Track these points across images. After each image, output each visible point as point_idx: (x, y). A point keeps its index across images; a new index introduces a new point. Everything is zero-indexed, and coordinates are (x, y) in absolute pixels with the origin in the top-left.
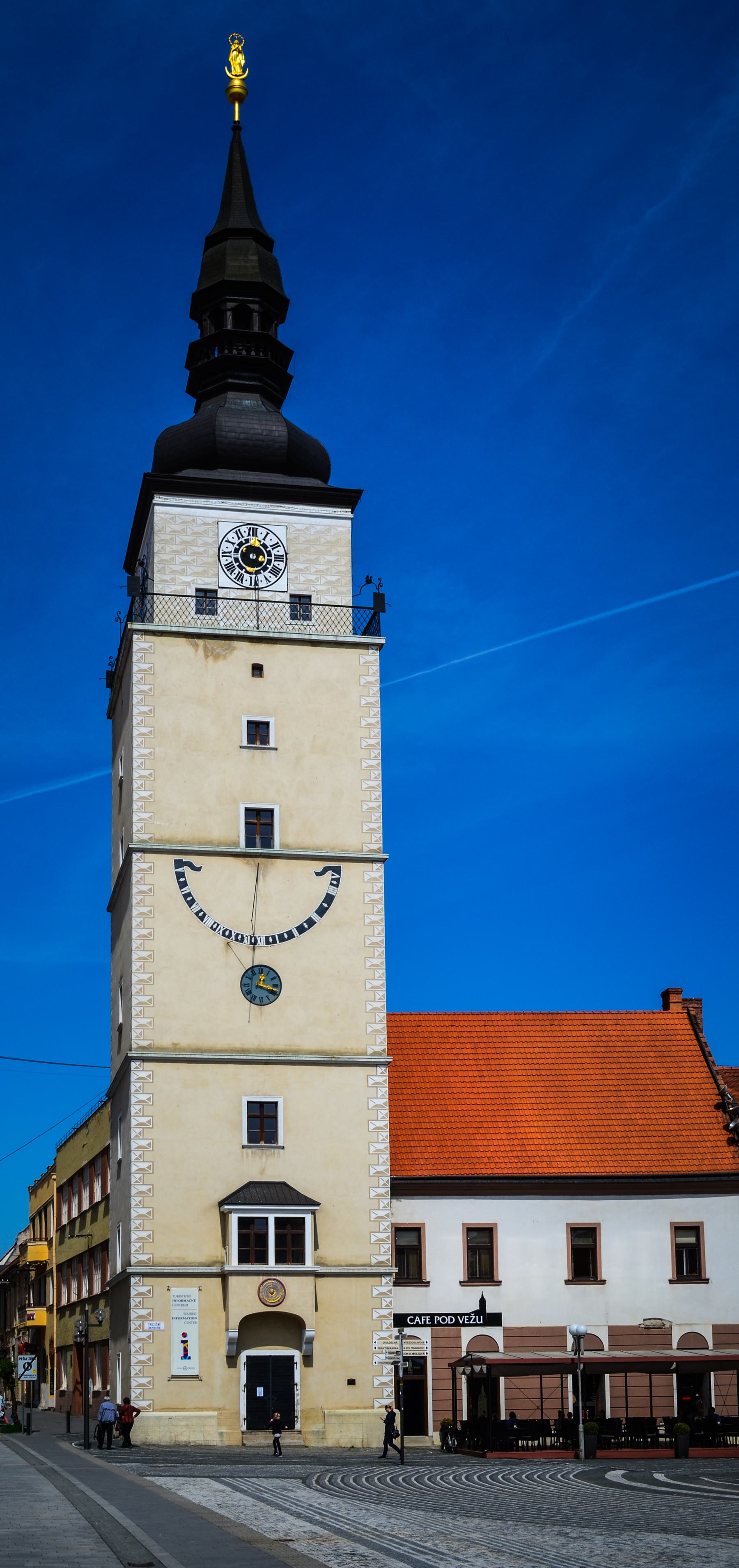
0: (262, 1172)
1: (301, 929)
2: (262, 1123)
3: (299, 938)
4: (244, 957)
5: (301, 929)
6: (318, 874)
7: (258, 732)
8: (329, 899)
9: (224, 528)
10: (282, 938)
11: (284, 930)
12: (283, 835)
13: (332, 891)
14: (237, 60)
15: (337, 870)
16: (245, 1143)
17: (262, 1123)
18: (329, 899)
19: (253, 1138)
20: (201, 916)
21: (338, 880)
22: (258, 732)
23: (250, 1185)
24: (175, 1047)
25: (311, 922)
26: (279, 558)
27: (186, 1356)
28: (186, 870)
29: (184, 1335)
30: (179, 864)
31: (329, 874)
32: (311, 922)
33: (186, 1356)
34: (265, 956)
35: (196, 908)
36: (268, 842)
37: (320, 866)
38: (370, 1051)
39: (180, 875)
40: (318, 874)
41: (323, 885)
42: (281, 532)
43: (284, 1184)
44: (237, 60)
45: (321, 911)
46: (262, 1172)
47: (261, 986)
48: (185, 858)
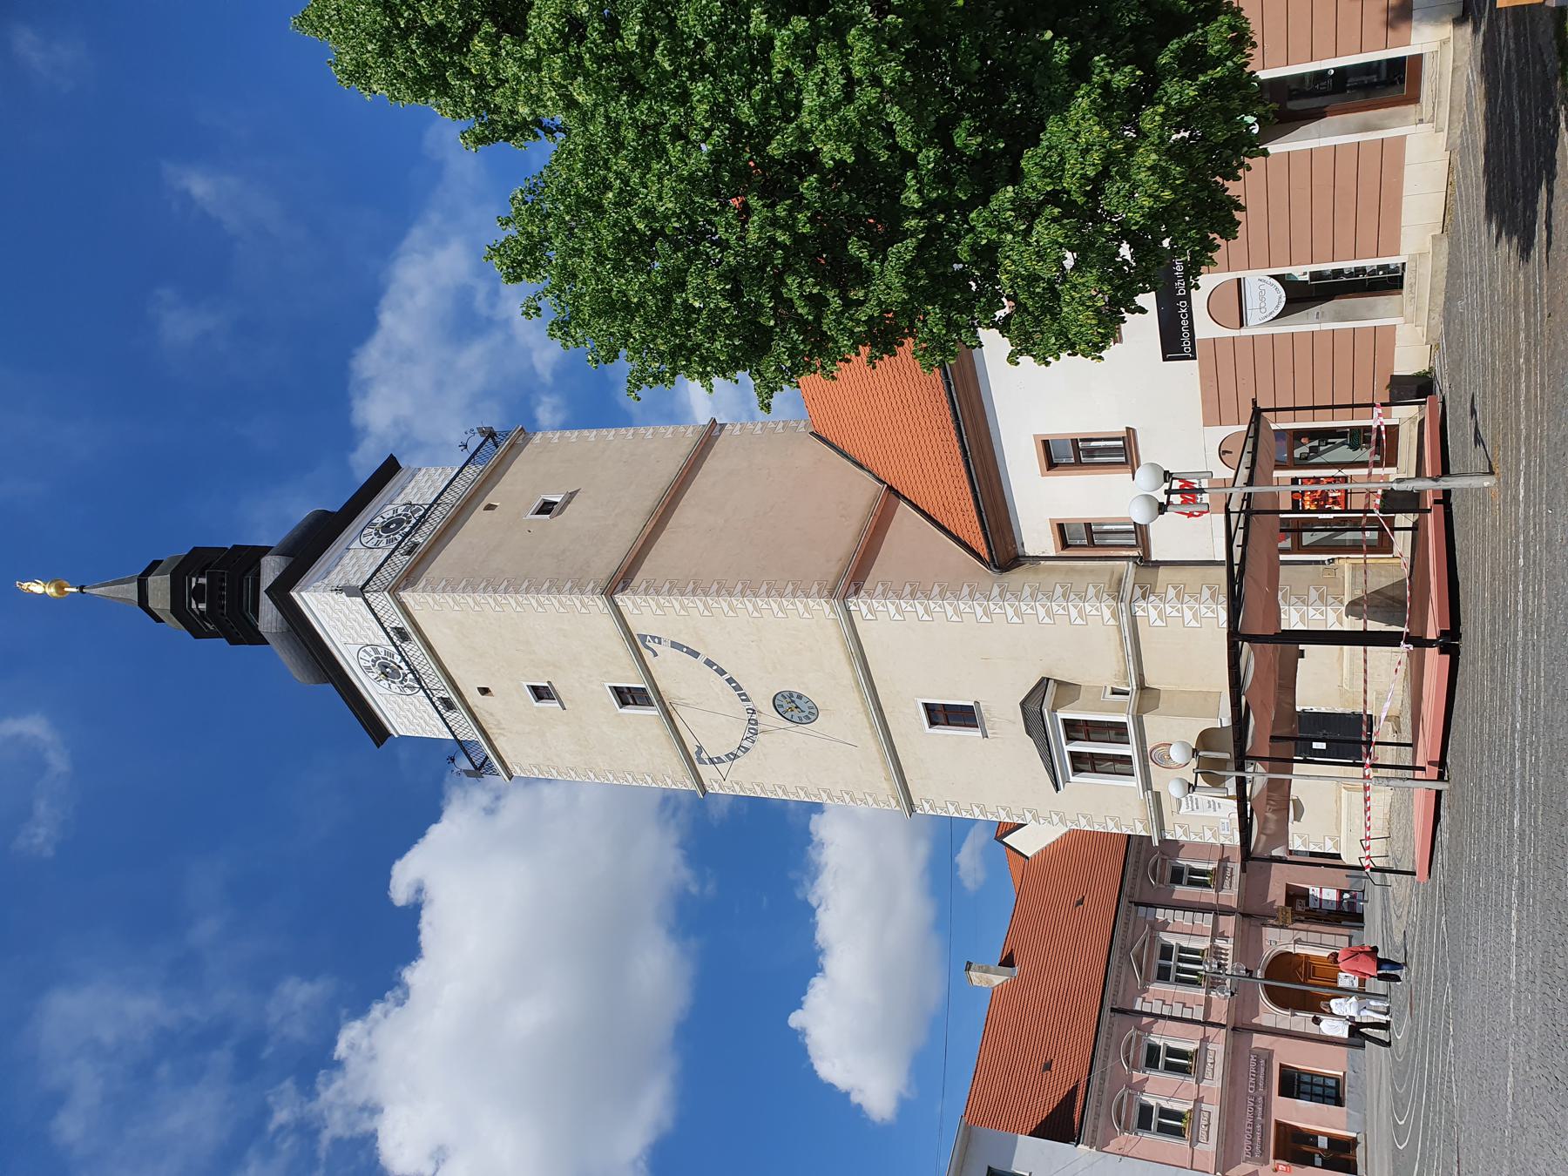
1: (721, 672)
3: (731, 673)
5: (721, 672)
6: (656, 655)
7: (540, 693)
8: (674, 645)
9: (382, 691)
10: (738, 688)
14: (37, 588)
15: (643, 638)
18: (674, 645)
22: (540, 693)
23: (1028, 733)
25: (709, 663)
26: (376, 652)
30: (702, 762)
31: (651, 645)
32: (709, 663)
37: (647, 654)
38: (832, 616)
40: (656, 655)
41: (664, 650)
44: (37, 588)
45: (696, 654)
47: (793, 707)
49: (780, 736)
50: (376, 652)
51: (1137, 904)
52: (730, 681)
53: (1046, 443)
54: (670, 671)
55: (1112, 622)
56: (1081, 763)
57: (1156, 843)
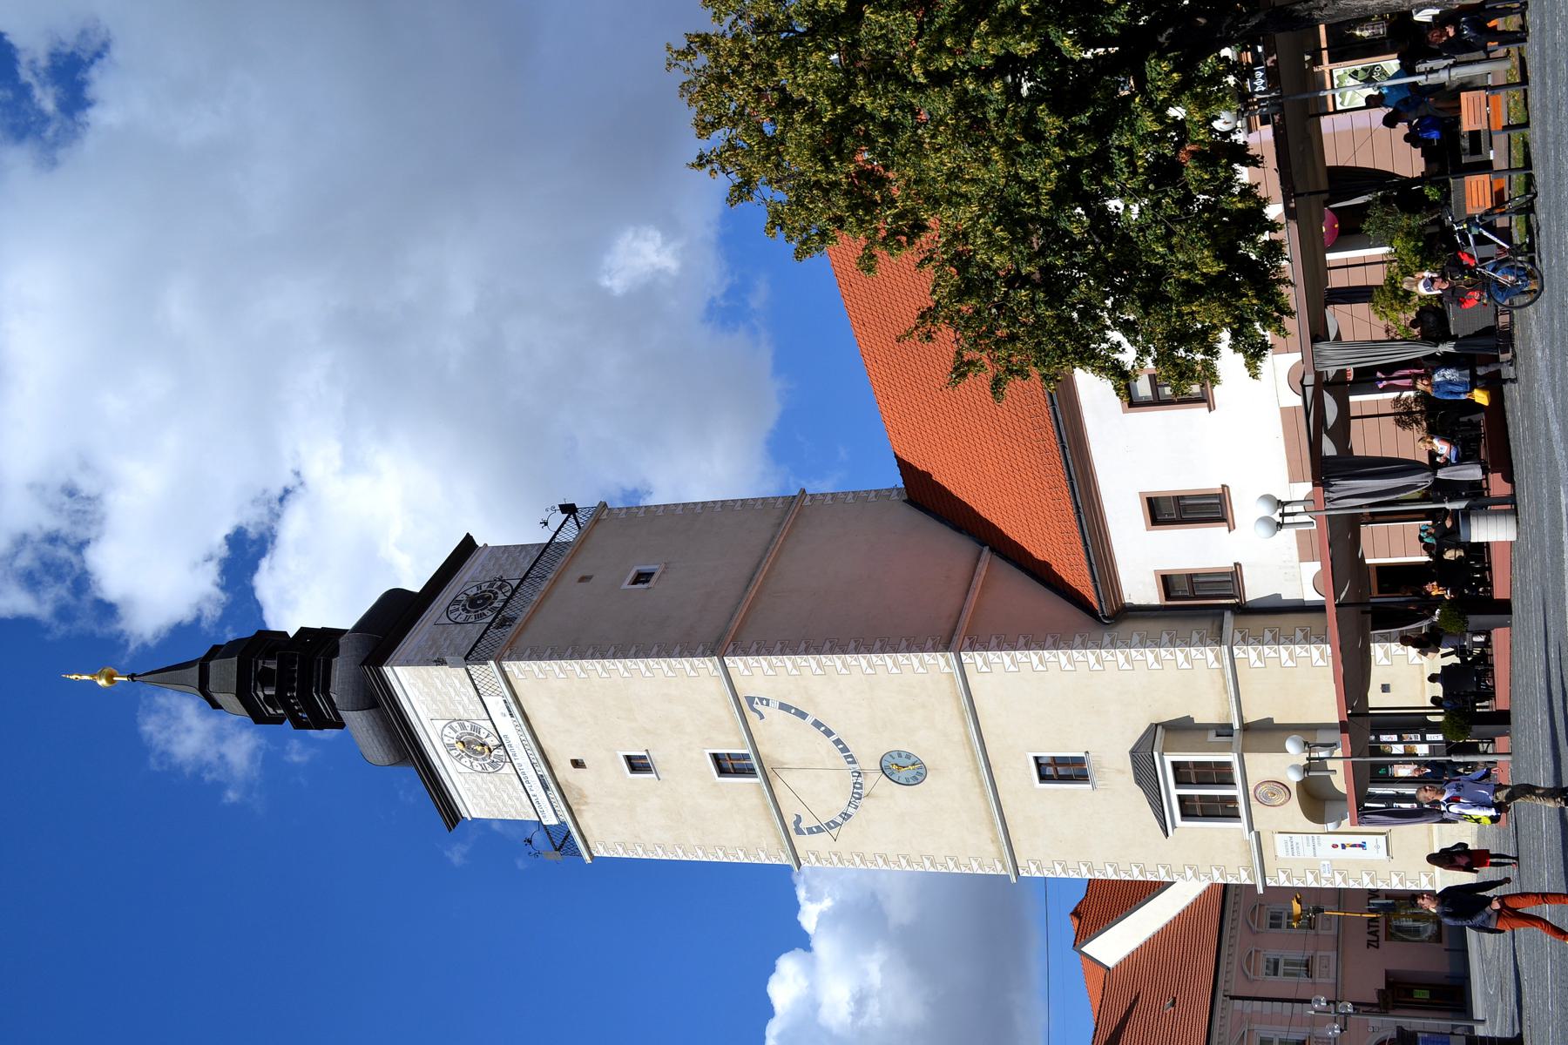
0: (1121, 772)
1: (828, 733)
2: (1062, 770)
3: (839, 733)
4: (875, 781)
5: (828, 733)
6: (762, 717)
7: (637, 765)
8: (783, 707)
10: (845, 750)
11: (835, 750)
12: (734, 745)
13: (774, 704)
15: (750, 700)
16: (1088, 786)
17: (1062, 770)
18: (784, 707)
19: (1082, 777)
20: (846, 816)
21: (761, 700)
22: (637, 765)
23: (1138, 782)
24: (995, 841)
25: (817, 724)
26: (463, 727)
27: (1362, 846)
28: (803, 826)
29: (1335, 846)
30: (799, 831)
31: (759, 707)
32: (817, 724)
33: (1362, 846)
34: (869, 762)
35: (839, 820)
36: (746, 757)
38: (947, 670)
39: (810, 831)
40: (762, 717)
41: (772, 712)
42: (440, 724)
43: (1133, 752)
45: (803, 715)
46: (1121, 772)
47: (903, 769)
48: (791, 828)
49: (888, 796)
50: (463, 727)
51: (1233, 998)
52: (838, 742)
53: (1149, 500)
54: (778, 738)
55: (1216, 665)
56: (1189, 809)
57: (1260, 890)
